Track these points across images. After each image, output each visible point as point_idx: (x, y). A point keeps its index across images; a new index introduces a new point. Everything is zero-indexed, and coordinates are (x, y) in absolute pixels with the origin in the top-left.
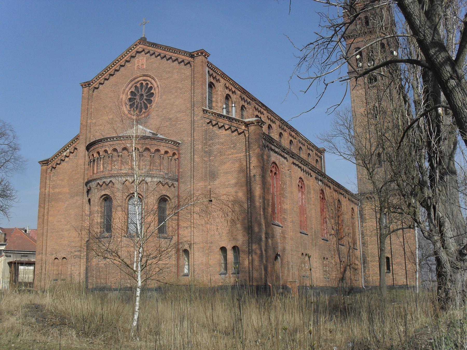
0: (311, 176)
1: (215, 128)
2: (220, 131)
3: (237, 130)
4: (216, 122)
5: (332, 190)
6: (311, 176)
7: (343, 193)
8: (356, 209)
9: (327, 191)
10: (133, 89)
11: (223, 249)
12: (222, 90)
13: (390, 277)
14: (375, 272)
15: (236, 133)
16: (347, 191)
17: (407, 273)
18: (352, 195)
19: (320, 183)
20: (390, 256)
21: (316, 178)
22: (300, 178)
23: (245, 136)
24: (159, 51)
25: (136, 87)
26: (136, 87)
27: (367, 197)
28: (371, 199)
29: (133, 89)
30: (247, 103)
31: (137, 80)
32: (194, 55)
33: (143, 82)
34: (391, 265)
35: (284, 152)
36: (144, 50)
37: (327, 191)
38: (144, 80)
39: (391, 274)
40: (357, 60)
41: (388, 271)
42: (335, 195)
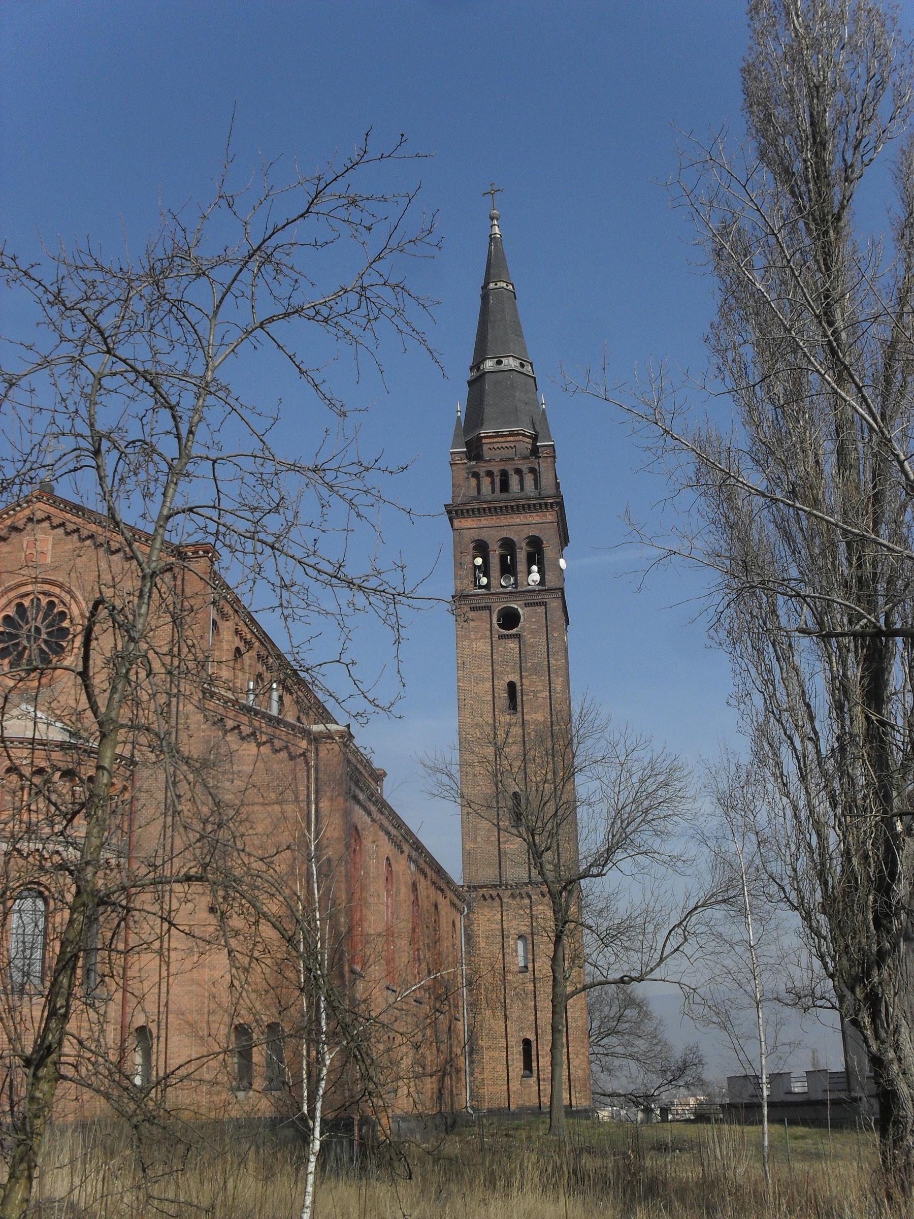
0: (402, 852)
1: (231, 738)
2: (245, 745)
3: (287, 747)
4: (236, 724)
5: (429, 882)
6: (402, 852)
7: (443, 886)
8: (460, 924)
9: (423, 884)
10: (11, 611)
11: (242, 1031)
12: (231, 639)
13: (530, 1086)
14: (496, 1075)
15: (283, 755)
16: (449, 882)
17: (572, 1077)
18: (455, 891)
19: (413, 867)
20: (532, 1037)
21: (410, 857)
22: (388, 859)
23: (307, 763)
24: (93, 527)
25: (20, 606)
26: (20, 606)
27: (483, 896)
28: (492, 898)
29: (11, 611)
30: (267, 668)
31: (24, 590)
32: (186, 554)
33: (40, 596)
34: (534, 1057)
35: (370, 800)
36: (48, 518)
37: (423, 884)
38: (44, 593)
39: (534, 1079)
40: (475, 566)
41: (527, 1072)
42: (432, 891)
